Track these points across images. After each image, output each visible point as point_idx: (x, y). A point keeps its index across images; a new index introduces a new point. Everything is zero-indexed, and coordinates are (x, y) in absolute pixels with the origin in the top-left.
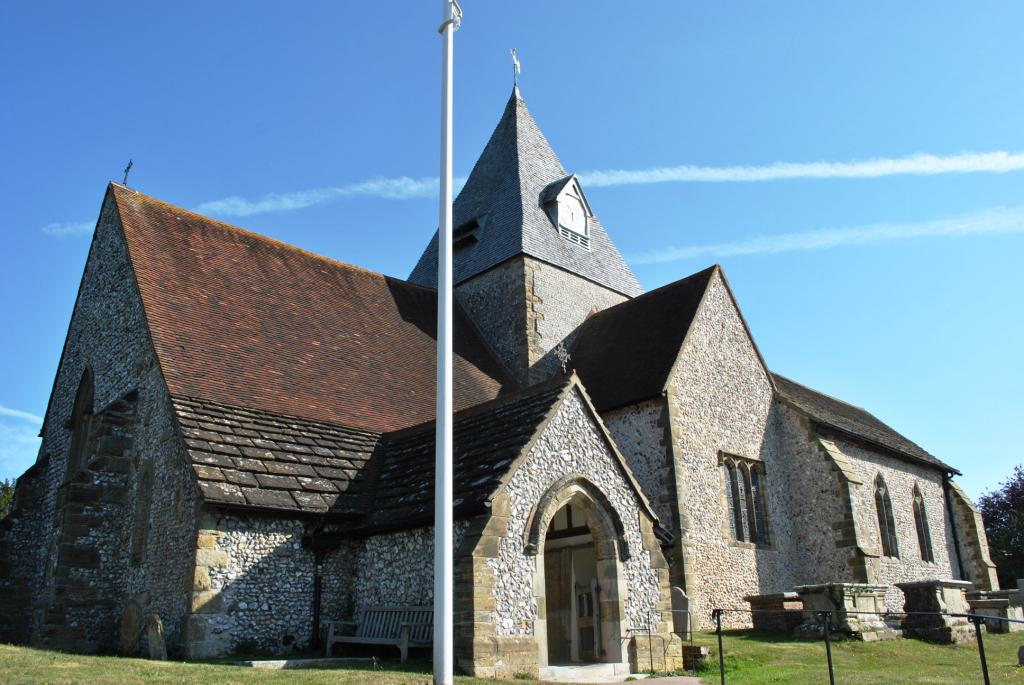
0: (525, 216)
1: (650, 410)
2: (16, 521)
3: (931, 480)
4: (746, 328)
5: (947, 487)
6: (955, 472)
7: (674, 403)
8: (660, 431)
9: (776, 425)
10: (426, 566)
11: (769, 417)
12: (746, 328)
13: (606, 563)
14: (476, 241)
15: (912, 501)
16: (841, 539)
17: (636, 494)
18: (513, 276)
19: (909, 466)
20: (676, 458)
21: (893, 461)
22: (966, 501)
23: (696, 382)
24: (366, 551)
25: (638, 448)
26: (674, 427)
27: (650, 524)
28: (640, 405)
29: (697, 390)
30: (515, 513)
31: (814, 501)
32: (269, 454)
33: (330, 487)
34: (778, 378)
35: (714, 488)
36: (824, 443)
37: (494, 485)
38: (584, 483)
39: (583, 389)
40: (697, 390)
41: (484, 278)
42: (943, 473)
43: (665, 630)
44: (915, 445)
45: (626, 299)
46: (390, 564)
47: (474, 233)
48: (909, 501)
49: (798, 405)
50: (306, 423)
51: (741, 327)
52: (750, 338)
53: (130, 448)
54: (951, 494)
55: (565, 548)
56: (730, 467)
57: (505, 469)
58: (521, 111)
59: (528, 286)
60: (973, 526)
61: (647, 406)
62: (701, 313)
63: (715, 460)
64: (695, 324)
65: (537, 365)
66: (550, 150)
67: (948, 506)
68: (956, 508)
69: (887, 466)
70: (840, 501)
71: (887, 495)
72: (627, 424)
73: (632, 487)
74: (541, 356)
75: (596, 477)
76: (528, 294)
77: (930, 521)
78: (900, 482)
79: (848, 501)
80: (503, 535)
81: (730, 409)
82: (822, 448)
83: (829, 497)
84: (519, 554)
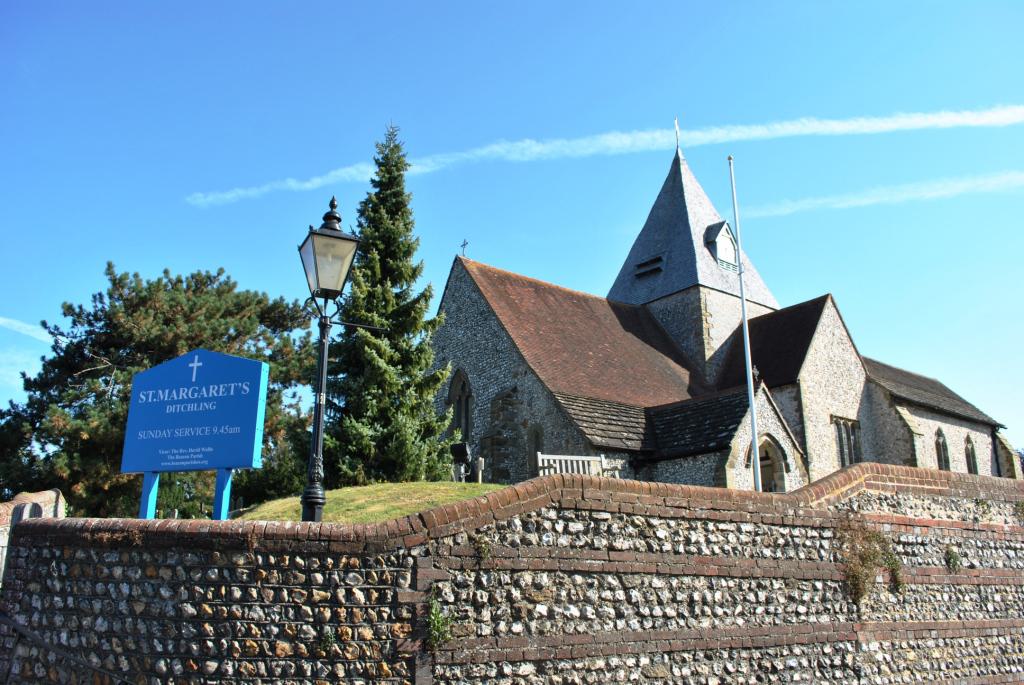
0: (697, 257)
1: (789, 390)
3: (982, 432)
4: (848, 334)
5: (994, 437)
7: (804, 386)
8: (795, 403)
9: (868, 396)
11: (863, 392)
12: (848, 334)
13: (778, 474)
15: (964, 447)
17: (792, 441)
18: (692, 299)
19: (964, 423)
20: (805, 419)
21: (951, 419)
22: (1009, 447)
23: (816, 372)
24: (657, 468)
26: (805, 401)
27: (799, 456)
29: (817, 378)
31: (892, 446)
32: (604, 421)
33: (635, 437)
35: (828, 437)
36: (899, 408)
37: (731, 437)
38: (769, 435)
39: (766, 389)
40: (817, 378)
41: (670, 299)
42: (992, 428)
44: (973, 407)
46: (674, 474)
47: (658, 265)
48: (962, 446)
49: (882, 384)
50: (611, 403)
51: (845, 334)
52: (851, 340)
53: (517, 417)
54: (997, 442)
56: (837, 424)
57: (735, 429)
58: (684, 168)
59: (703, 306)
60: (1012, 465)
62: (820, 328)
63: (828, 420)
64: (816, 336)
65: (711, 358)
66: (706, 197)
67: (995, 450)
68: (1001, 452)
69: (946, 422)
70: (908, 445)
73: (790, 437)
74: (712, 353)
76: (703, 312)
77: (978, 461)
78: (955, 434)
79: (913, 446)
81: (838, 388)
82: (897, 412)
83: (901, 443)
84: (743, 467)
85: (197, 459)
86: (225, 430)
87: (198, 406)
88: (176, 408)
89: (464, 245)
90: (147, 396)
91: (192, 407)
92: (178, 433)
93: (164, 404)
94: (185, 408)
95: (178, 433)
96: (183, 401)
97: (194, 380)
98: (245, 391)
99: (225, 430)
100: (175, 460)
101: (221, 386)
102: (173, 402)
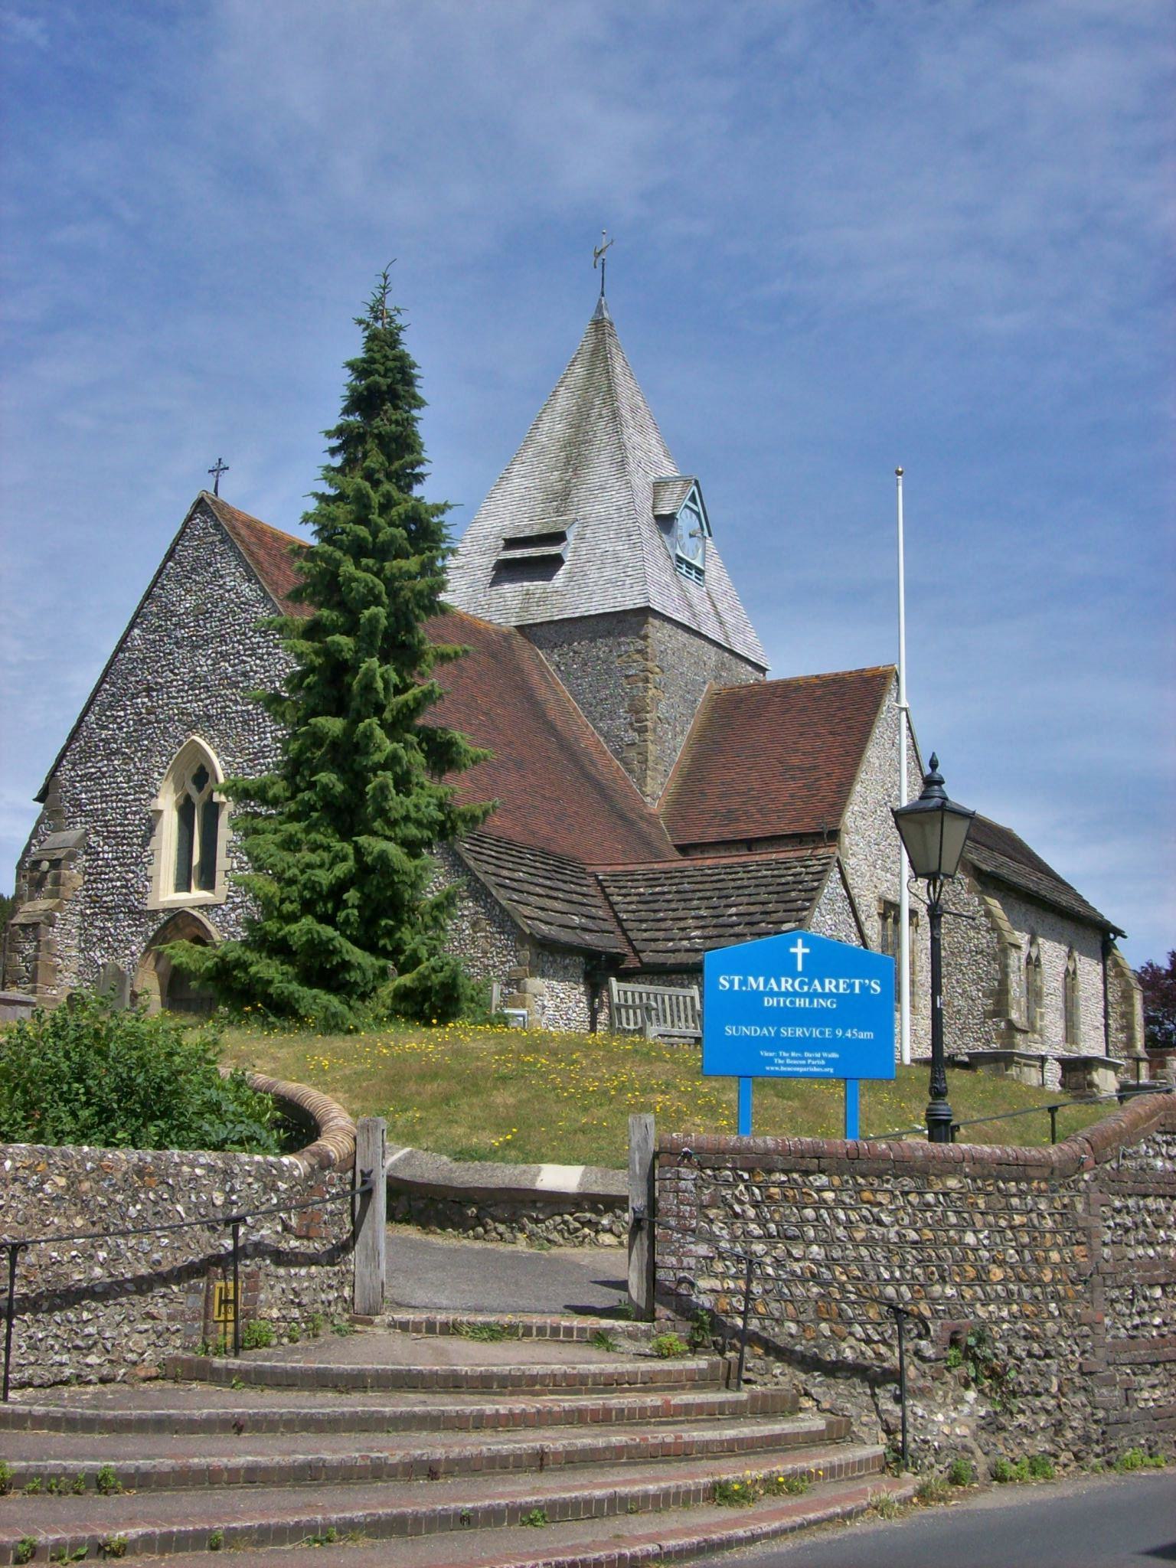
2: (58, 914)
6: (1119, 933)
16: (991, 1008)
36: (989, 900)
71: (1038, 959)
85: (817, 1066)
86: (853, 1035)
87: (811, 1002)
88: (778, 1002)
89: (219, 469)
90: (732, 983)
91: (800, 1003)
92: (786, 1032)
93: (758, 996)
94: (792, 1002)
95: (786, 1032)
96: (787, 994)
97: (800, 968)
98: (875, 990)
99: (853, 1035)
100: (785, 1065)
101: (841, 981)
102: (772, 994)
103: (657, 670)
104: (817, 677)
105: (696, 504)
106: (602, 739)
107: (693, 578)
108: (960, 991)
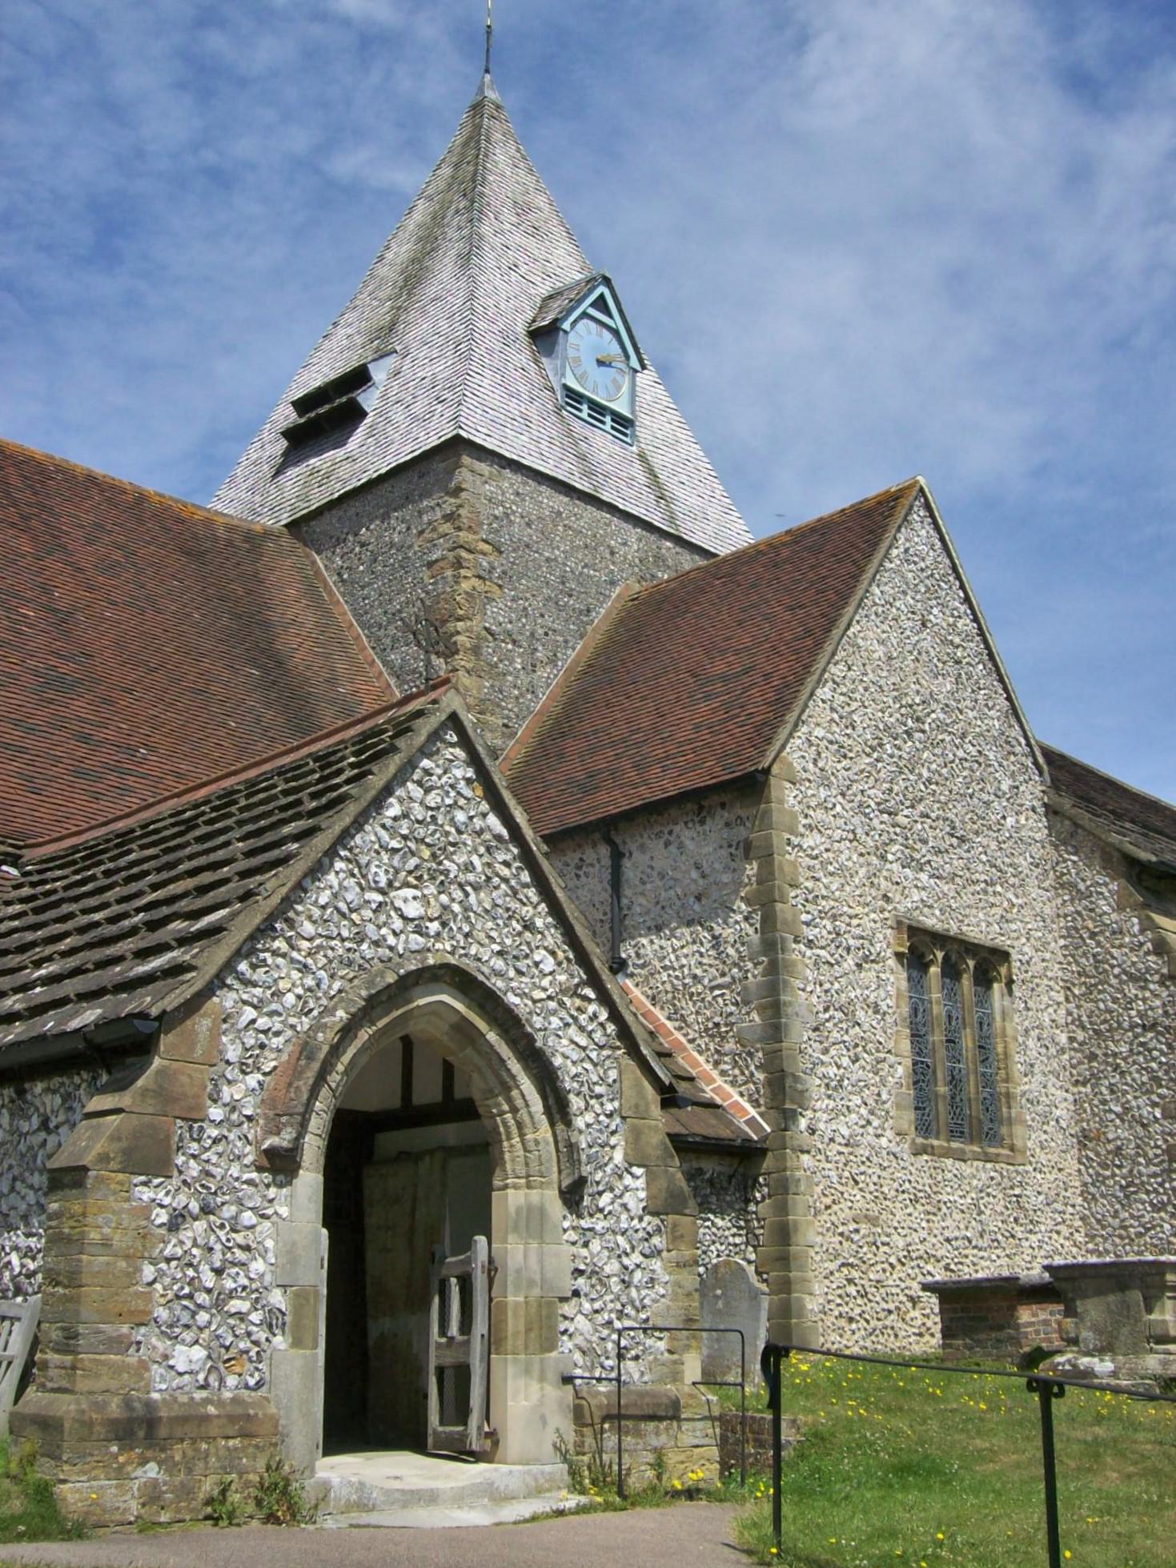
10: (13, 1189)
14: (364, 414)
25: (697, 907)
28: (705, 803)
30: (233, 1053)
34: (1049, 754)
43: (676, 1376)
45: (702, 562)
55: (431, 1152)
61: (723, 805)
72: (673, 848)
75: (499, 963)
80: (194, 1119)
103: (486, 548)
104: (788, 532)
105: (610, 316)
106: (392, 682)
107: (608, 427)
108: (1118, 1109)
